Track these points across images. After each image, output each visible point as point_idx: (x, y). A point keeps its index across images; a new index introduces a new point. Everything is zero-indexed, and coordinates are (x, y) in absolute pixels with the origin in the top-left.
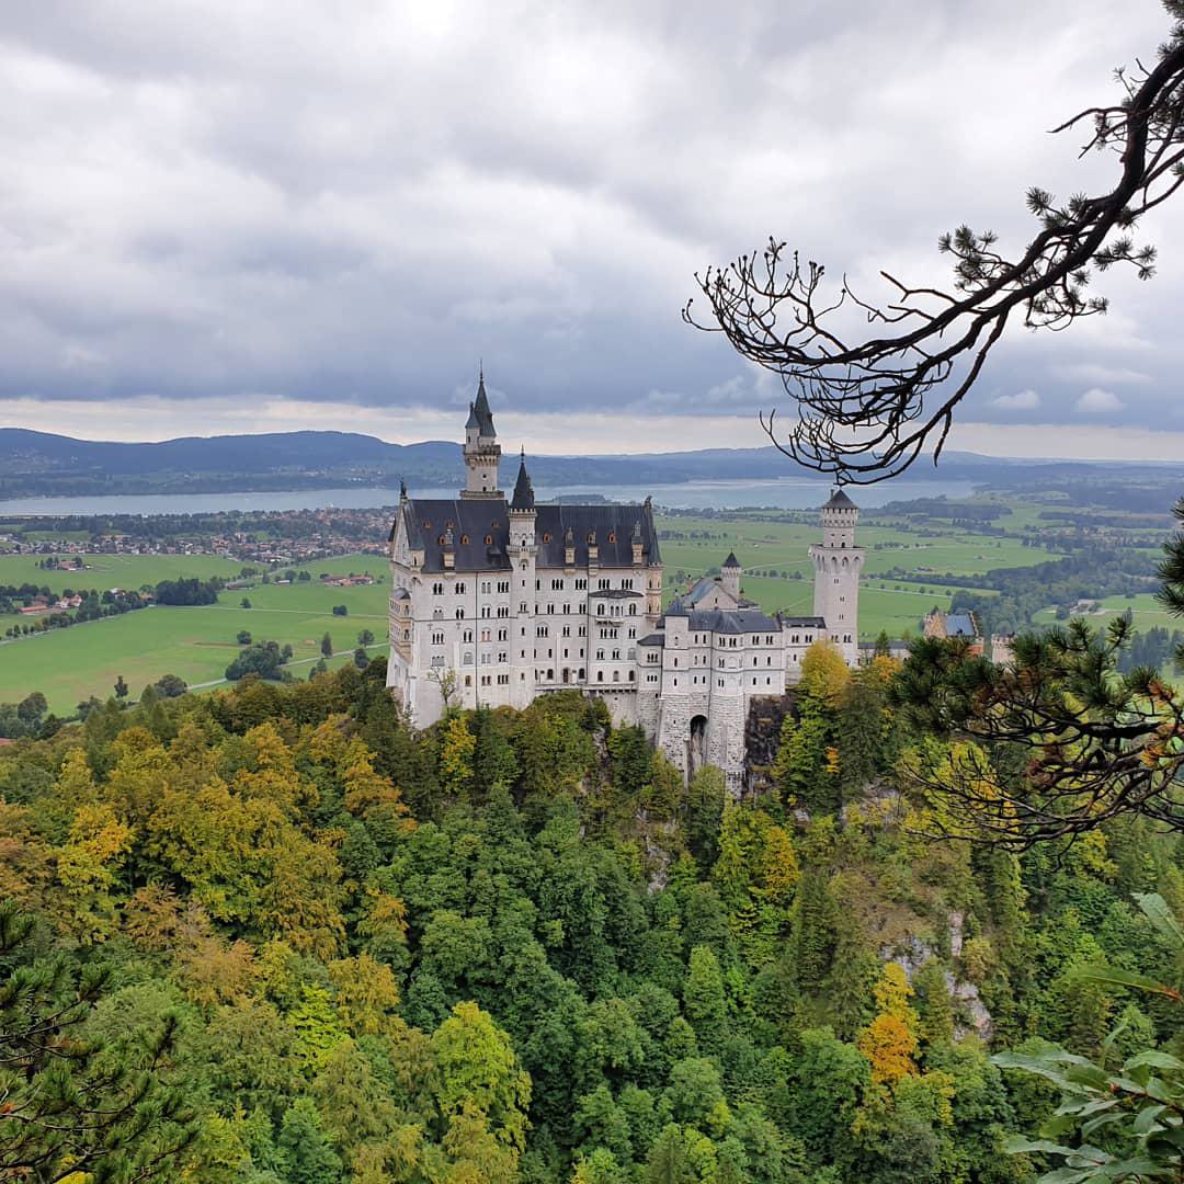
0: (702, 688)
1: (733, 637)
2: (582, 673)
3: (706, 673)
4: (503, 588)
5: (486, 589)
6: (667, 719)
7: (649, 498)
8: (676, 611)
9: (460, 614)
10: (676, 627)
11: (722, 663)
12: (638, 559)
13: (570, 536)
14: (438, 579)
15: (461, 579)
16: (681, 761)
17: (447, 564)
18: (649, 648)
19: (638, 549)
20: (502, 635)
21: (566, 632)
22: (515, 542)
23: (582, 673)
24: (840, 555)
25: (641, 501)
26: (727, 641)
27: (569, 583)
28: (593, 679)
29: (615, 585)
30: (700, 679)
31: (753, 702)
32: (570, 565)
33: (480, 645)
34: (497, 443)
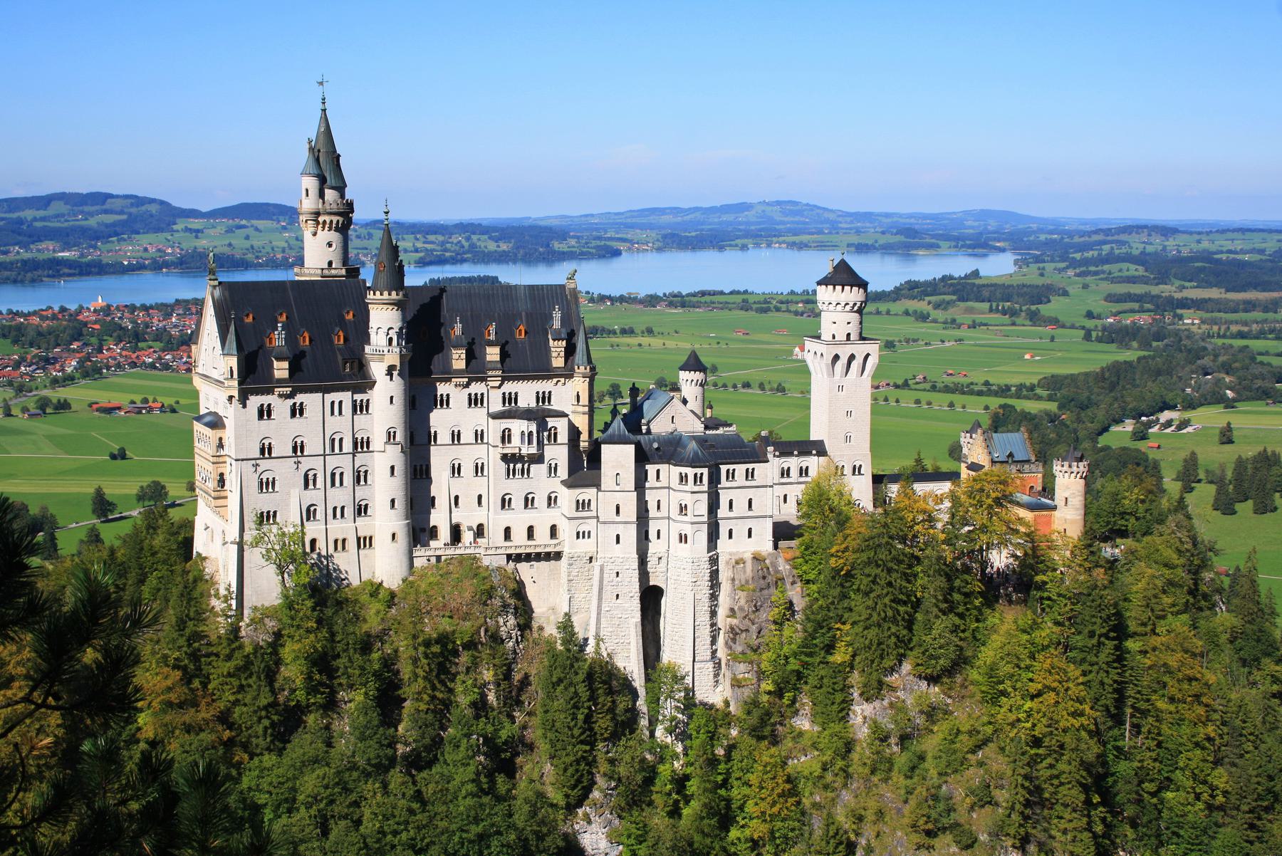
1: (699, 471)
5: (336, 409)
9: (298, 449)
12: (558, 362)
13: (458, 329)
15: (300, 398)
18: (578, 491)
19: (557, 349)
20: (360, 477)
21: (456, 470)
23: (480, 531)
32: (459, 373)
33: (330, 491)
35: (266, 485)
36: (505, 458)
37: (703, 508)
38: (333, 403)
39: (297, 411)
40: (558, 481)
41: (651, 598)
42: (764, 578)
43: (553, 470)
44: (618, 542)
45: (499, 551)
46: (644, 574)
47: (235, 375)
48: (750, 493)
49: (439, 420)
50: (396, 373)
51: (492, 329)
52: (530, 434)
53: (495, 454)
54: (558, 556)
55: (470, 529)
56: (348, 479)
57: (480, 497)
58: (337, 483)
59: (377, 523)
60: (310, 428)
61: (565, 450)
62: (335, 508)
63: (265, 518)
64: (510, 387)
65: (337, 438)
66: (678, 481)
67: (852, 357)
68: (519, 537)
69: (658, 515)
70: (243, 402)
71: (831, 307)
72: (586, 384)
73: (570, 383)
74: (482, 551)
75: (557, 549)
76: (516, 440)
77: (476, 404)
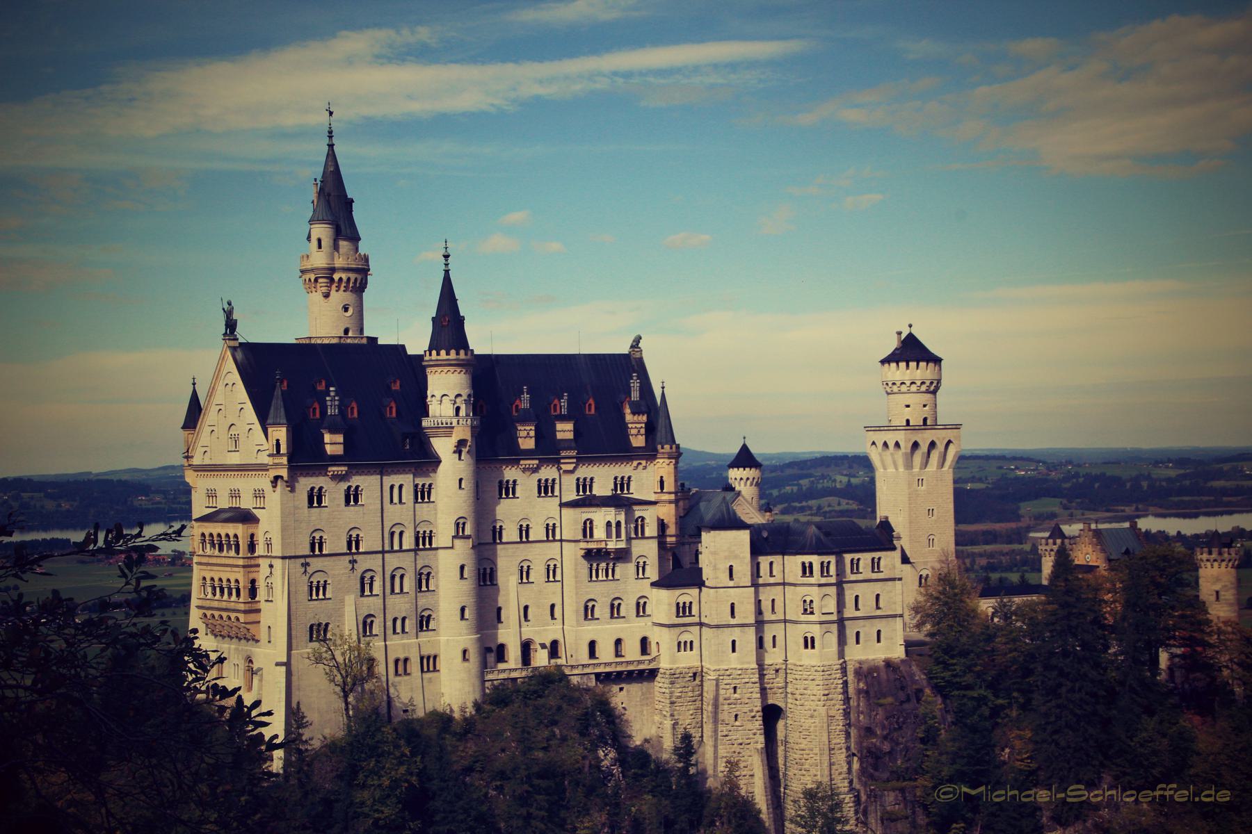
1: (826, 559)
6: (726, 714)
7: (638, 340)
9: (353, 543)
12: (638, 441)
13: (525, 401)
15: (356, 481)
16: (755, 787)
17: (329, 449)
18: (678, 592)
19: (635, 424)
20: (423, 579)
21: (524, 574)
24: (925, 438)
25: (624, 349)
26: (816, 568)
28: (584, 657)
29: (602, 488)
31: (859, 673)
32: (528, 454)
33: (391, 600)
35: (317, 589)
36: (589, 555)
37: (832, 606)
38: (392, 487)
39: (352, 497)
41: (771, 715)
42: (903, 688)
43: (641, 568)
44: (734, 650)
46: (763, 691)
47: (283, 450)
48: (877, 588)
49: (508, 513)
50: (465, 450)
51: (564, 403)
54: (649, 675)
55: (543, 646)
56: (409, 584)
57: (553, 606)
58: (397, 590)
59: (443, 639)
61: (654, 545)
62: (395, 620)
63: (318, 632)
64: (585, 471)
65: (397, 530)
66: (800, 573)
67: (932, 445)
69: (773, 617)
70: (291, 485)
72: (672, 466)
73: (651, 467)
74: (567, 672)
75: (651, 667)
76: (599, 533)
77: (546, 492)
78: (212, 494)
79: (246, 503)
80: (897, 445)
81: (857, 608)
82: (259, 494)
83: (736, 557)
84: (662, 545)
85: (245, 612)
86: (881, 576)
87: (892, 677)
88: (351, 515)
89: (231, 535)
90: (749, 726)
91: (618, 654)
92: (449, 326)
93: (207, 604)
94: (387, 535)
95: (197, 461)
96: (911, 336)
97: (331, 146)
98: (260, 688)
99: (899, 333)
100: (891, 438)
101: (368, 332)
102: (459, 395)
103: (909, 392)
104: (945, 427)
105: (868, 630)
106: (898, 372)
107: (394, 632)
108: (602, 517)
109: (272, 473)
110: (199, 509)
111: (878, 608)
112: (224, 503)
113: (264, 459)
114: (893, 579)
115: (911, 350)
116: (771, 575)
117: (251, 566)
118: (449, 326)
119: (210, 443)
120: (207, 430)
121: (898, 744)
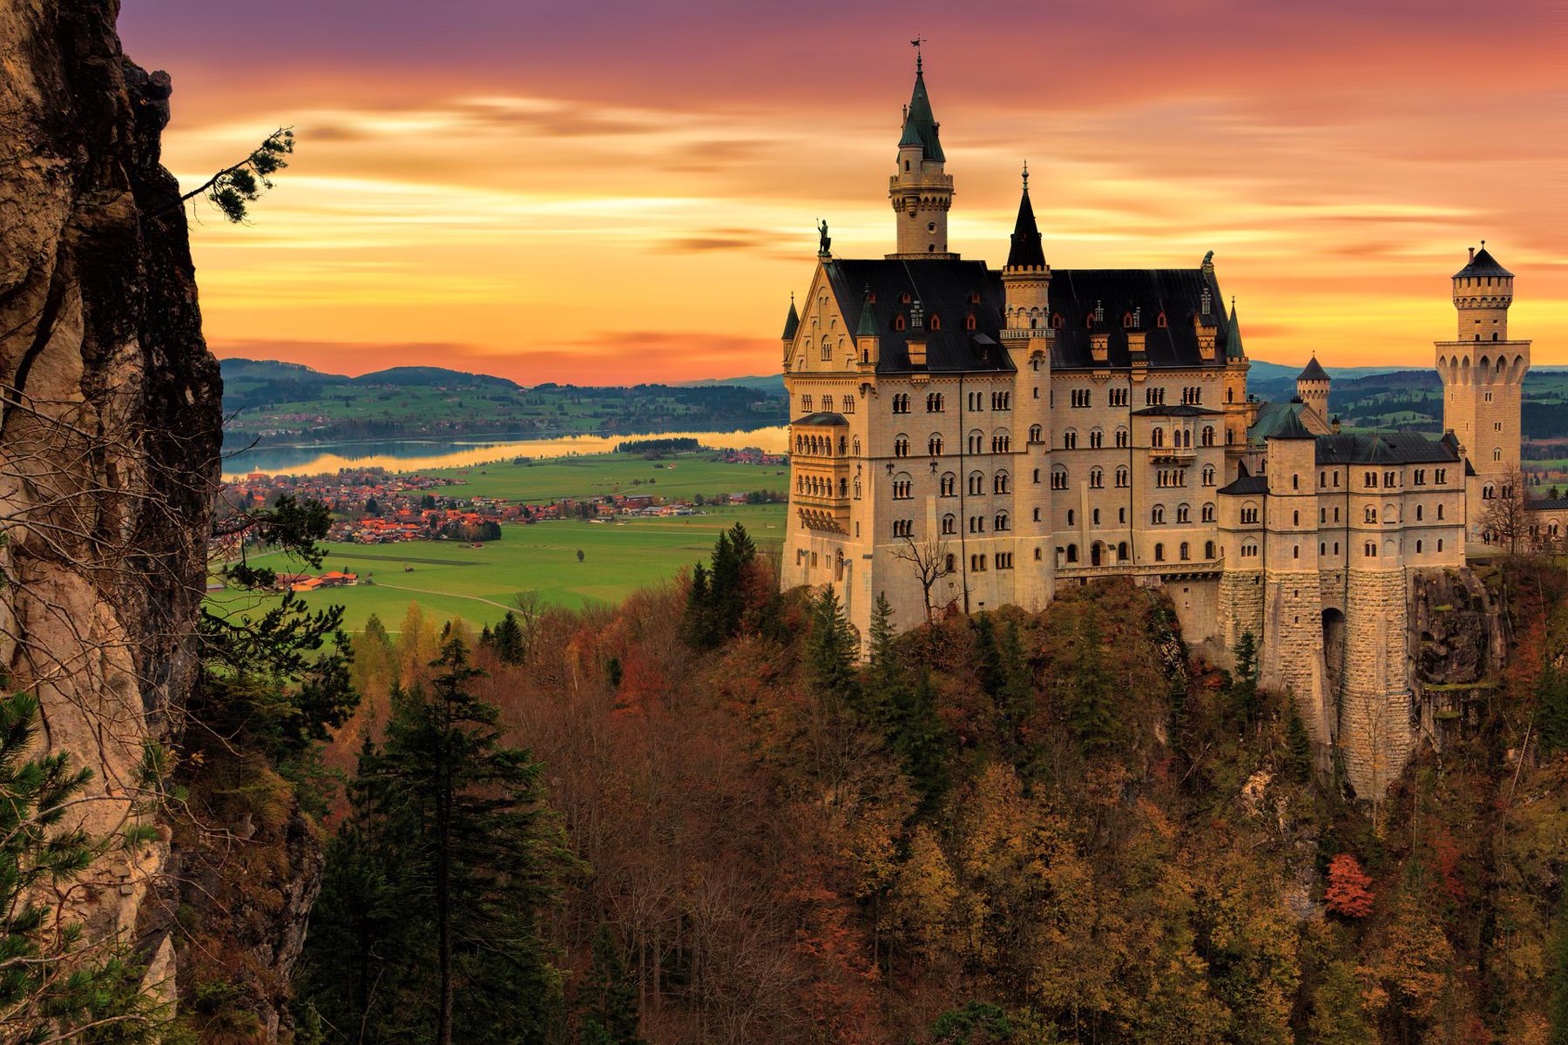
0: (1335, 563)
1: (1390, 470)
2: (1123, 551)
3: (1340, 538)
4: (1001, 402)
5: (975, 402)
7: (1210, 255)
8: (1294, 432)
9: (935, 447)
10: (1287, 462)
11: (1371, 516)
12: (1208, 353)
14: (901, 387)
16: (1313, 687)
17: (914, 360)
18: (1243, 499)
19: (1205, 337)
20: (1002, 484)
21: (1096, 480)
22: (1017, 323)
24: (1494, 354)
26: (1380, 478)
27: (1099, 395)
28: (1150, 558)
29: (1173, 399)
30: (1330, 548)
31: (1417, 581)
32: (1102, 365)
34: (946, 172)
35: (902, 490)
37: (1393, 515)
40: (1213, 489)
41: (1331, 618)
43: (1208, 477)
45: (1153, 572)
48: (1440, 499)
51: (1136, 316)
52: (1187, 433)
53: (1141, 460)
55: (1112, 547)
56: (987, 486)
57: (1122, 510)
60: (945, 426)
61: (1221, 454)
63: (903, 529)
67: (1502, 359)
68: (1172, 556)
71: (1475, 305)
73: (1220, 379)
76: (1168, 442)
78: (807, 400)
79: (838, 408)
80: (1466, 360)
81: (1419, 518)
82: (849, 401)
83: (1301, 467)
84: (1230, 455)
85: (836, 508)
86: (1444, 487)
87: (1451, 584)
88: (934, 422)
89: (824, 436)
90: (1309, 628)
91: (1184, 556)
92: (1026, 242)
93: (803, 500)
94: (966, 441)
95: (794, 369)
96: (1483, 252)
97: (920, 74)
98: (850, 577)
99: (1471, 250)
100: (1460, 353)
101: (949, 250)
102: (1035, 309)
103: (1479, 308)
104: (1515, 344)
105: (1430, 540)
106: (1472, 290)
107: (972, 530)
108: (1170, 426)
109: (861, 381)
110: (796, 412)
111: (1440, 518)
112: (817, 408)
113: (856, 369)
114: (1458, 491)
115: (1482, 265)
116: (1336, 485)
117: (842, 466)
118: (1026, 242)
119: (808, 356)
120: (803, 341)
121: (1453, 649)
